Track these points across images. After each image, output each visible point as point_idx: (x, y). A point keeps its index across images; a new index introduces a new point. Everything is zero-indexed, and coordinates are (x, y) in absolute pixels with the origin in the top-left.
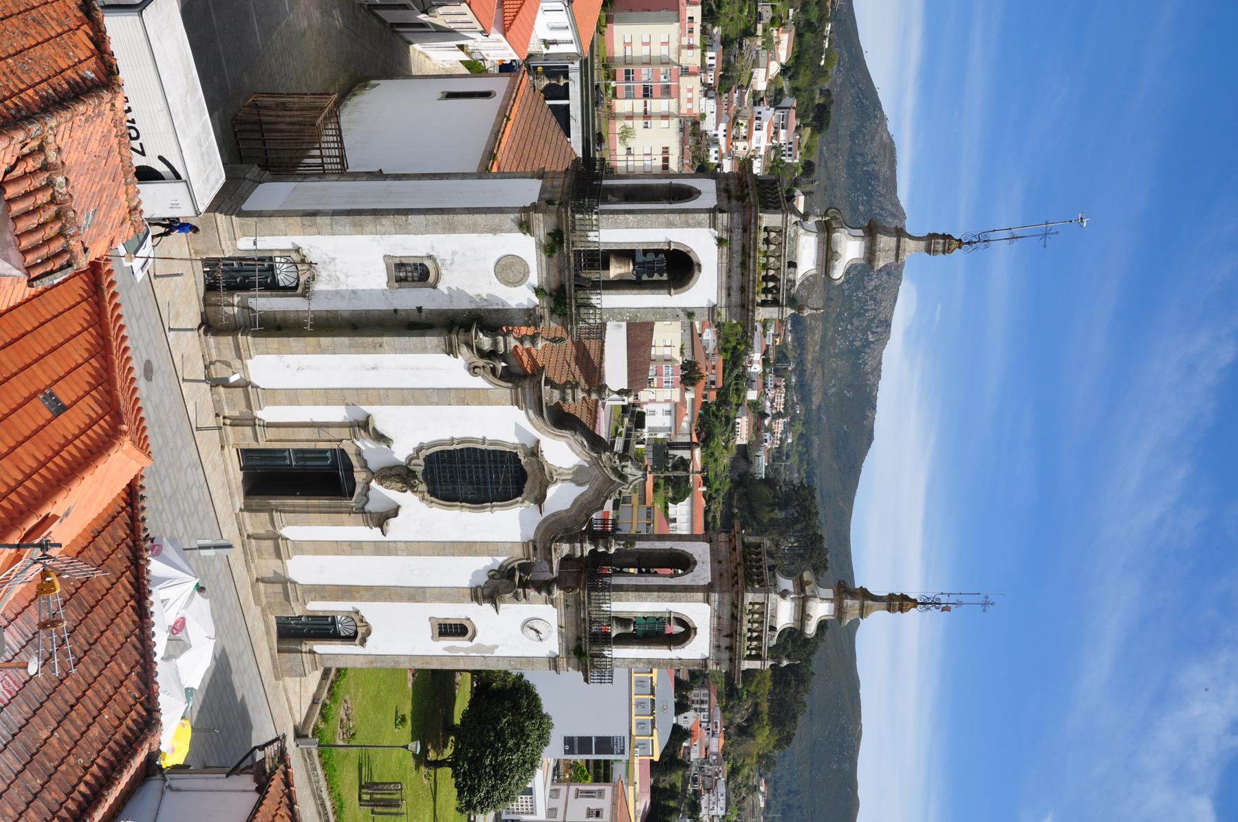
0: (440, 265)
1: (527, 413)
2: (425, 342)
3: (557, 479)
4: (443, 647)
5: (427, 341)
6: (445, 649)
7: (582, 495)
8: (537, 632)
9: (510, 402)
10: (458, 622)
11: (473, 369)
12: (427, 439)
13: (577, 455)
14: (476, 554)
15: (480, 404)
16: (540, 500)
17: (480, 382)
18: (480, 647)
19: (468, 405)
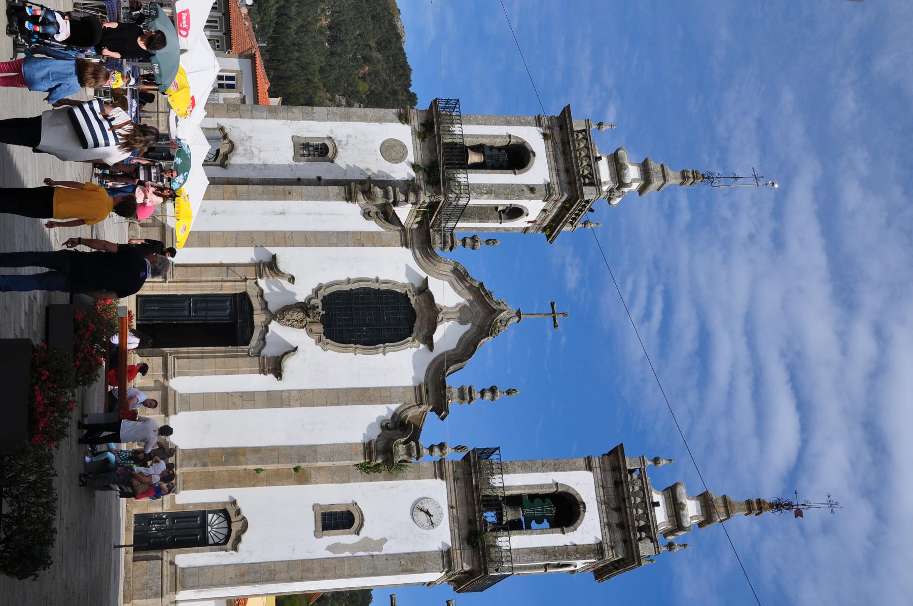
0: (337, 145)
1: (414, 253)
2: (328, 191)
3: (442, 319)
4: (325, 546)
5: (330, 189)
6: (329, 548)
7: (467, 332)
8: (427, 513)
9: (400, 243)
10: (344, 509)
11: (367, 215)
12: (325, 281)
13: (459, 293)
14: (371, 401)
15: (374, 245)
16: (428, 341)
17: (372, 226)
18: (367, 543)
19: (363, 246)
